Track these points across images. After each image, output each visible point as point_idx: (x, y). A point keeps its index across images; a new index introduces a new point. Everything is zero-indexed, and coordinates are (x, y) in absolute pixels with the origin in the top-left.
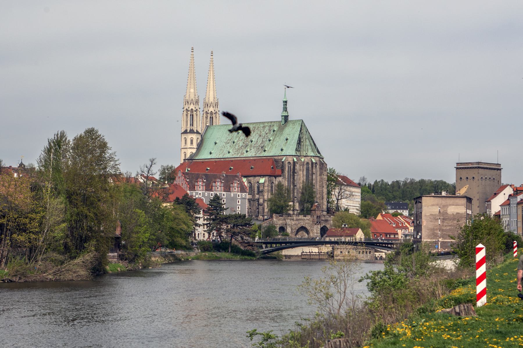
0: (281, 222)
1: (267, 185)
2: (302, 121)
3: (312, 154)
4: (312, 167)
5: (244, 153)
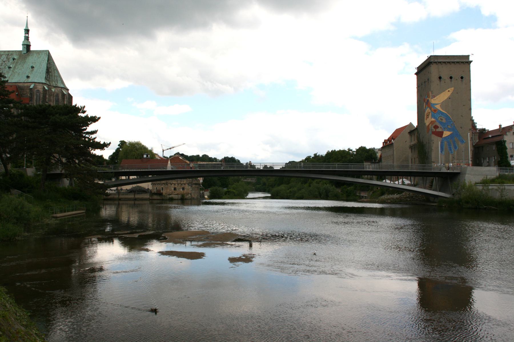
2: (49, 52)
3: (62, 86)
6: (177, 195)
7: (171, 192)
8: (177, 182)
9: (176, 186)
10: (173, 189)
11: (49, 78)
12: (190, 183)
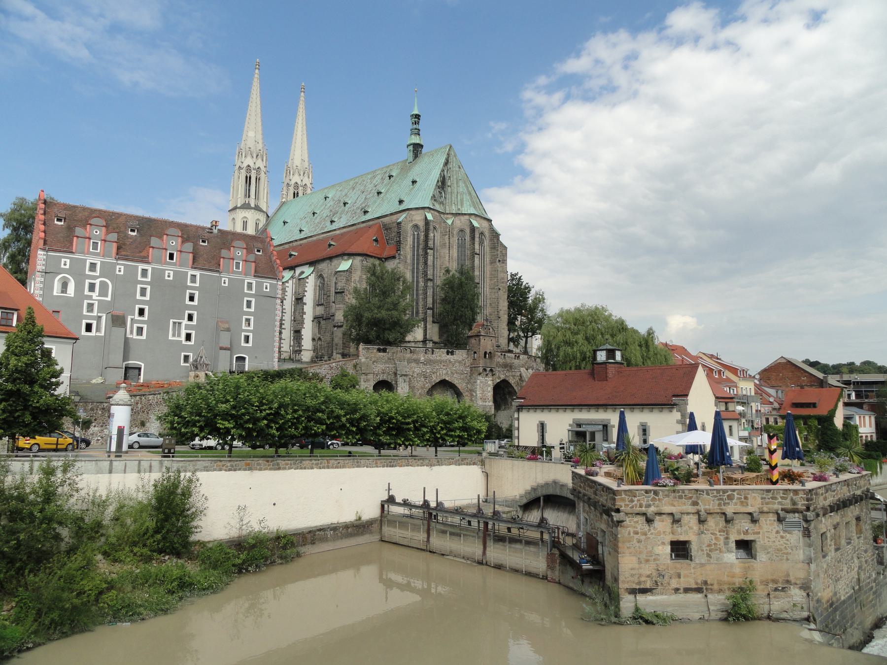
0: (379, 367)
1: (357, 279)
3: (472, 211)
4: (473, 238)
5: (326, 227)
6: (700, 595)
7: (648, 569)
8: (695, 504)
9: (688, 532)
10: (668, 548)
11: (445, 198)
12: (794, 511)
